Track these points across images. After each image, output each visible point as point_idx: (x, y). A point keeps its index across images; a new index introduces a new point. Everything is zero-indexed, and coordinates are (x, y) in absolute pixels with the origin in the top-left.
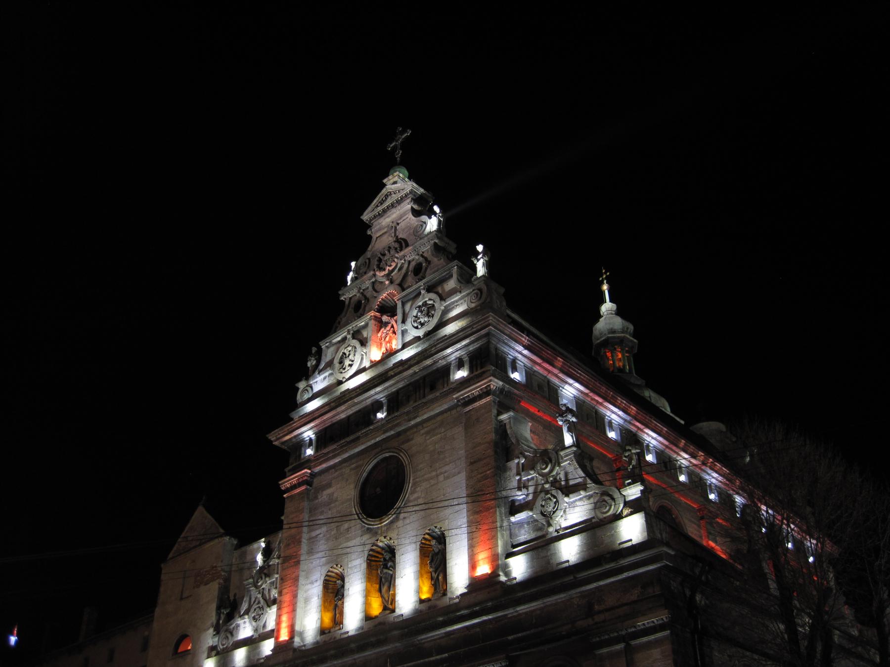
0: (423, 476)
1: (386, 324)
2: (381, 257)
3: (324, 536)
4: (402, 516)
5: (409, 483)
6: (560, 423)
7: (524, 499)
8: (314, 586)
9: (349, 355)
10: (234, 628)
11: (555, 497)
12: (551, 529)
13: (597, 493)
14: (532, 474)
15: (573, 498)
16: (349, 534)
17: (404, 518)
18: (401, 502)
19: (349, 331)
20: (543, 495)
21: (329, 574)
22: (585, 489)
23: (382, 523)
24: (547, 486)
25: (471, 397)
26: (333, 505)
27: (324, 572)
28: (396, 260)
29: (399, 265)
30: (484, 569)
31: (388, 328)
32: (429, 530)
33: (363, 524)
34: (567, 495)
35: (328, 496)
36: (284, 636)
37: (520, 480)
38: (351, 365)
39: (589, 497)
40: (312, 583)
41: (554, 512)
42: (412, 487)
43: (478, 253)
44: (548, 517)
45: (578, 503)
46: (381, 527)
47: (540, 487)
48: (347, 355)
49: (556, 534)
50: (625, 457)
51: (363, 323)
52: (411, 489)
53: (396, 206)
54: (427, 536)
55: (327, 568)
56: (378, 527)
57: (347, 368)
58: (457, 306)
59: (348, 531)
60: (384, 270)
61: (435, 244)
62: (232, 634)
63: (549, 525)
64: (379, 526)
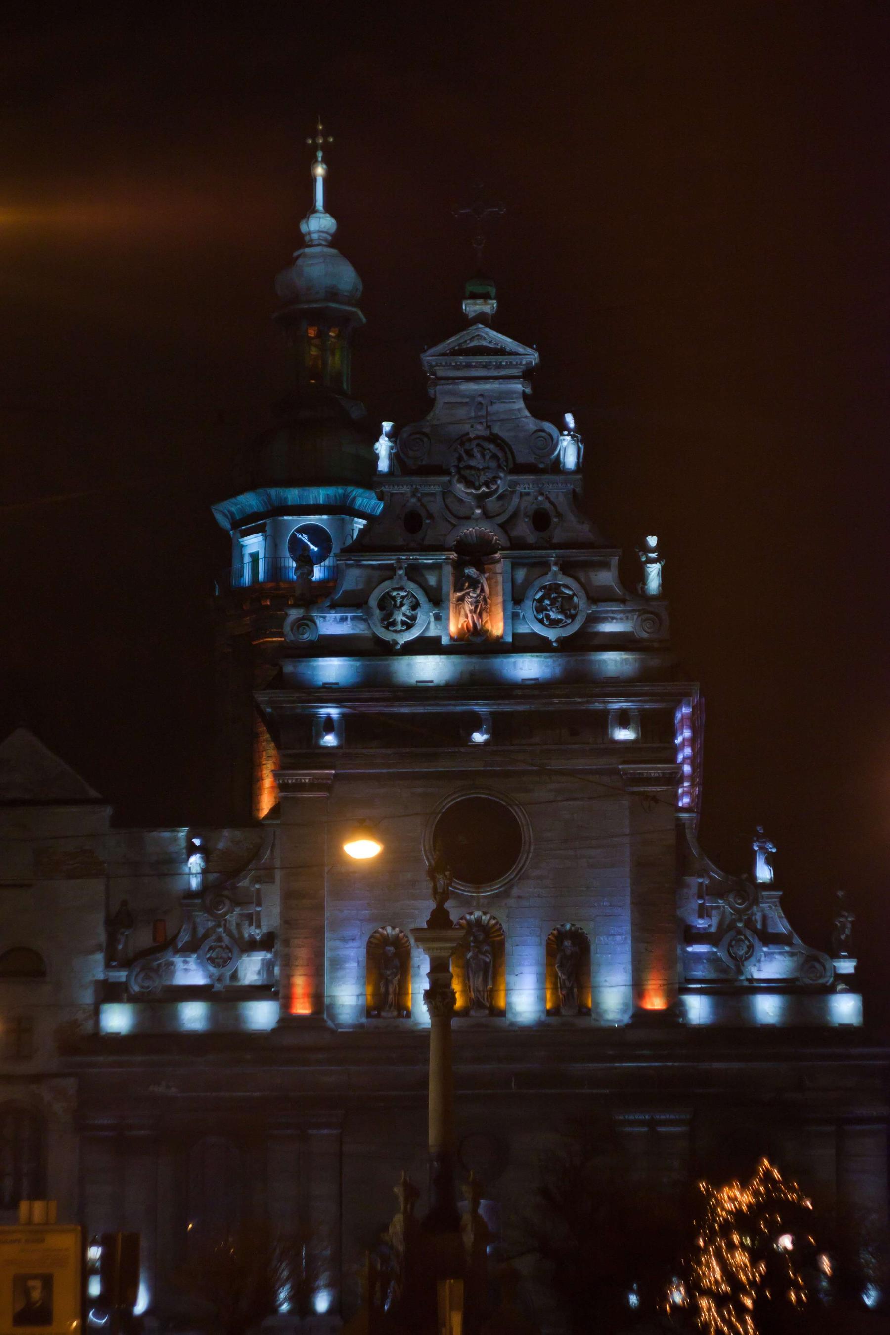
1: (474, 584)
2: (464, 456)
4: (515, 891)
6: (756, 849)
7: (704, 928)
9: (402, 605)
10: (160, 965)
11: (749, 941)
12: (742, 978)
13: (803, 954)
14: (720, 903)
15: (773, 949)
18: (515, 874)
19: (399, 560)
20: (732, 933)
22: (790, 944)
23: (479, 893)
24: (740, 925)
25: (645, 775)
27: (368, 929)
28: (499, 482)
29: (501, 491)
30: (656, 1002)
31: (478, 592)
32: (562, 925)
34: (766, 944)
36: (302, 1008)
37: (701, 906)
38: (409, 626)
39: (791, 954)
40: (344, 940)
41: (746, 959)
43: (647, 549)
44: (739, 963)
45: (777, 957)
47: (727, 921)
48: (398, 604)
49: (746, 984)
50: (840, 922)
51: (430, 561)
53: (491, 369)
54: (555, 932)
57: (399, 627)
58: (613, 618)
60: (477, 489)
61: (574, 490)
62: (157, 970)
63: (740, 972)
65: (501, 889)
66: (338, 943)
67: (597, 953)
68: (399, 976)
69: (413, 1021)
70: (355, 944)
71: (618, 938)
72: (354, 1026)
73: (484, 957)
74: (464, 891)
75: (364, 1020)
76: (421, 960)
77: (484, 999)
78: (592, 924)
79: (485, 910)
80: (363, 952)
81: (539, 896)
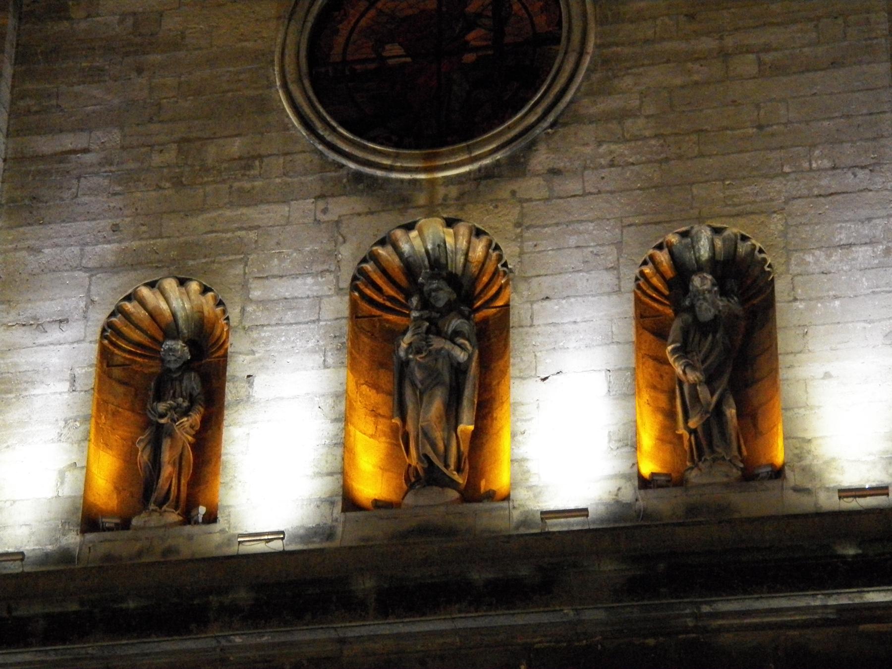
0: (646, 41)
3: (107, 161)
4: (541, 159)
5: (581, 54)
8: (43, 339)
16: (254, 178)
17: (555, 172)
18: (540, 110)
21: (129, 306)
26: (156, 58)
32: (684, 235)
33: (332, 156)
35: (130, 21)
40: (37, 325)
42: (589, 71)
46: (432, 182)
52: (587, 77)
54: (663, 257)
55: (120, 283)
56: (414, 182)
59: (249, 167)
64: (422, 176)
65: (498, 156)
66: (19, 336)
67: (795, 299)
68: (196, 417)
69: (222, 531)
70: (72, 332)
71: (862, 253)
72: (46, 558)
73: (448, 346)
74: (391, 169)
75: (73, 539)
76: (260, 359)
77: (447, 466)
78: (776, 224)
79: (451, 213)
80: (90, 351)
81: (612, 164)
